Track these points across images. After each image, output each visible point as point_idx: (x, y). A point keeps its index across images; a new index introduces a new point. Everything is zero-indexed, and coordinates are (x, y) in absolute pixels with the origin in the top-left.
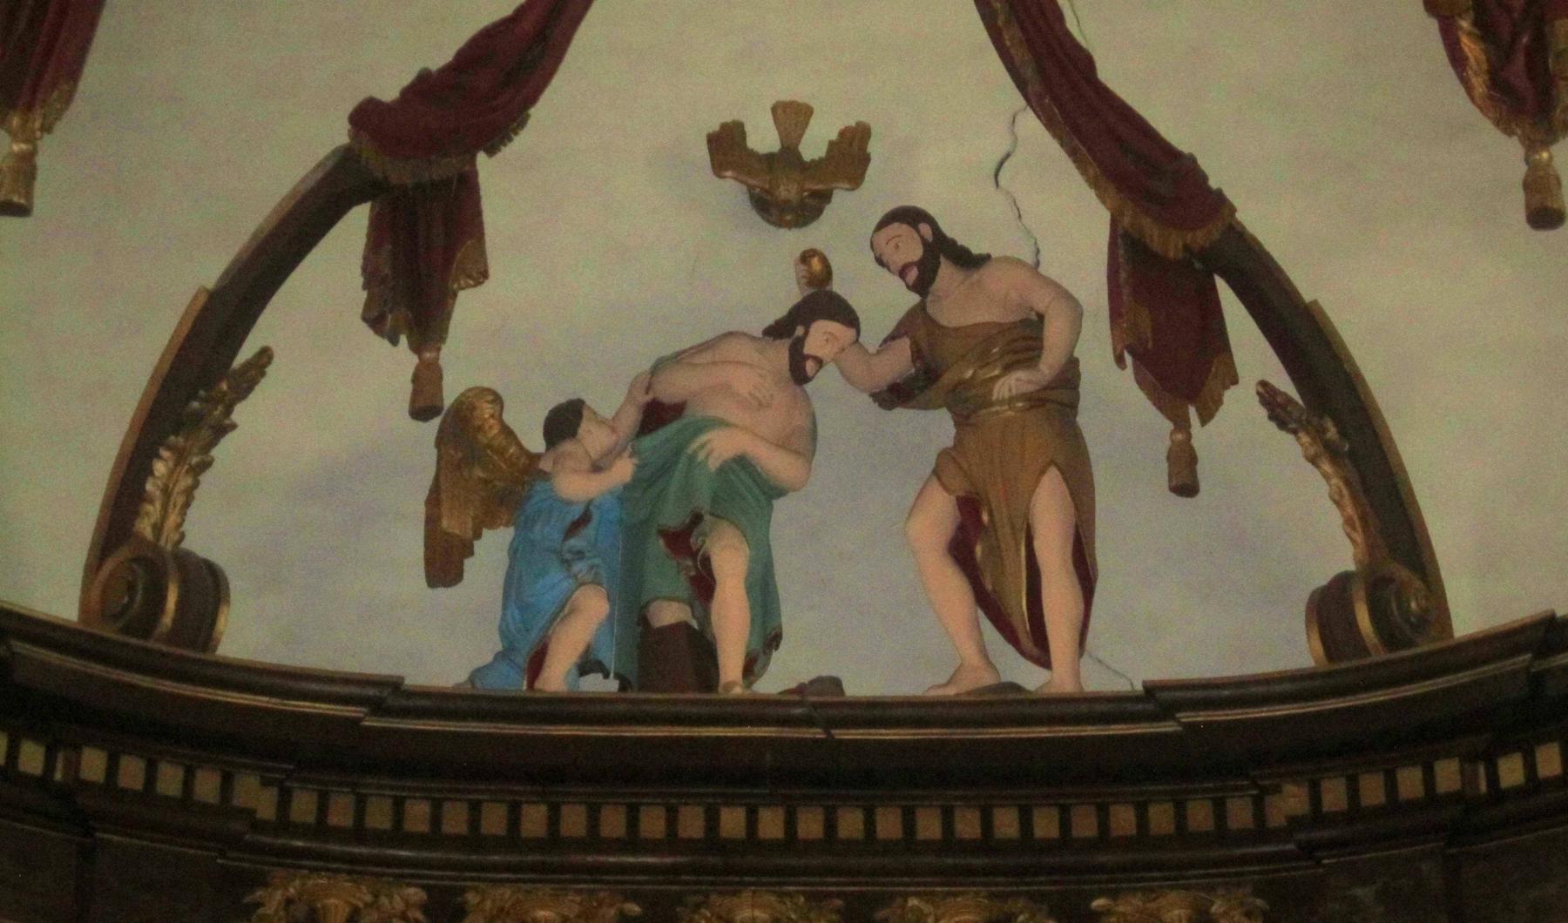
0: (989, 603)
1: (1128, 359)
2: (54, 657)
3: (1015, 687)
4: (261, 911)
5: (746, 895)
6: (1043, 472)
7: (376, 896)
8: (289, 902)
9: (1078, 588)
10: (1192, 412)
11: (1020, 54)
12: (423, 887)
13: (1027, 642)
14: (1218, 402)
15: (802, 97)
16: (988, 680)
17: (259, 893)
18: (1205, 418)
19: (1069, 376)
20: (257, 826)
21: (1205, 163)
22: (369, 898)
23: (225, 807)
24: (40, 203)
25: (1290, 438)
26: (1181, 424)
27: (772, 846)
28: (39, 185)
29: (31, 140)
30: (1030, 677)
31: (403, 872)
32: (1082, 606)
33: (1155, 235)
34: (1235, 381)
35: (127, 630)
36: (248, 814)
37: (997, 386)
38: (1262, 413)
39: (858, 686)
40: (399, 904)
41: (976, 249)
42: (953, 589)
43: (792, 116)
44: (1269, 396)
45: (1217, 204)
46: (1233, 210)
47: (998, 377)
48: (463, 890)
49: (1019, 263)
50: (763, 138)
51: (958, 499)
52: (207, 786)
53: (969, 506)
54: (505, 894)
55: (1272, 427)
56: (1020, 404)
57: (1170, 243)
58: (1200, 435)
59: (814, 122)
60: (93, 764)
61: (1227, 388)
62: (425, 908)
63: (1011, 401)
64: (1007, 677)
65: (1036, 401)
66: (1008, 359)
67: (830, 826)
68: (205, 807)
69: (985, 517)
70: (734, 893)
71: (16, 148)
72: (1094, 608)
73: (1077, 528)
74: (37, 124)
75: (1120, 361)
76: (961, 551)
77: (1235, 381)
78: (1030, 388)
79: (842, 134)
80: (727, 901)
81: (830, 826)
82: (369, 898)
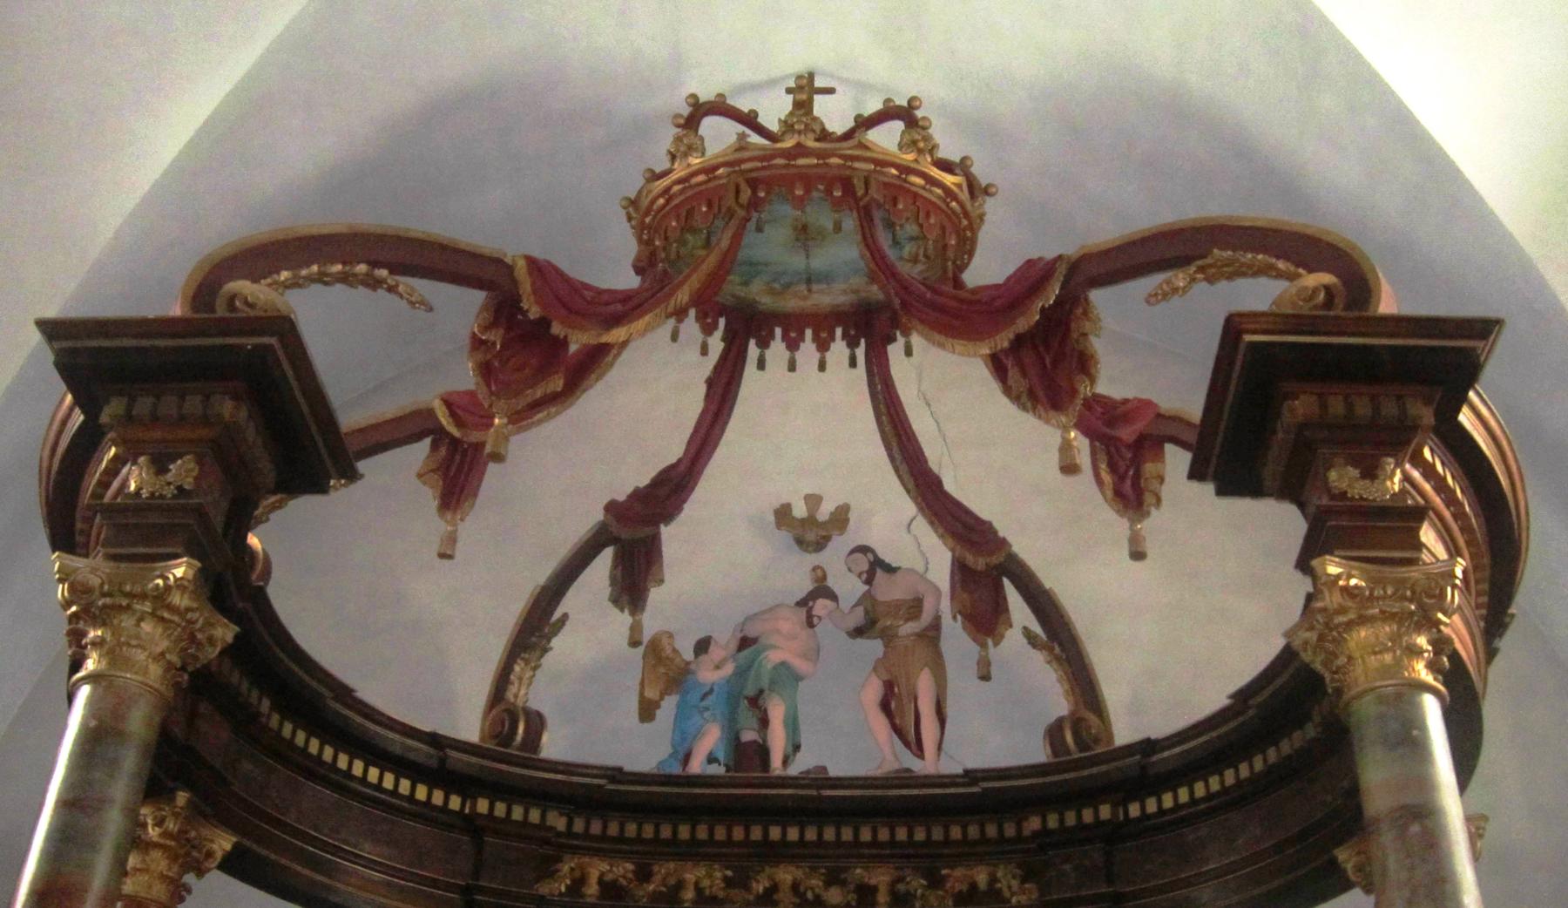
0: (898, 730)
1: (959, 617)
2: (465, 757)
3: (908, 770)
4: (558, 874)
5: (782, 866)
6: (922, 670)
7: (611, 866)
8: (572, 869)
9: (938, 725)
10: (990, 642)
11: (906, 477)
12: (633, 863)
13: (913, 746)
14: (1002, 637)
15: (817, 492)
16: (896, 766)
17: (561, 865)
18: (996, 644)
19: (936, 626)
20: (559, 834)
21: (997, 525)
22: (608, 868)
23: (542, 826)
24: (459, 555)
25: (1039, 652)
26: (983, 646)
27: (793, 844)
28: (459, 545)
29: (455, 525)
30: (920, 767)
31: (626, 855)
32: (939, 734)
33: (970, 559)
34: (1011, 626)
35: (498, 745)
36: (552, 829)
37: (901, 628)
38: (1025, 641)
39: (833, 772)
40: (622, 871)
41: (894, 565)
42: (880, 724)
43: (813, 501)
44: (1028, 633)
45: (1003, 543)
46: (1010, 546)
47: (901, 625)
48: (650, 865)
49: (916, 573)
50: (800, 511)
51: (884, 682)
52: (535, 816)
53: (889, 686)
54: (672, 865)
55: (1029, 647)
56: (912, 638)
57: (979, 563)
58: (994, 652)
59: (824, 503)
60: (483, 806)
61: (1007, 629)
62: (633, 872)
63: (908, 636)
64: (906, 765)
65: (921, 635)
66: (907, 616)
67: (820, 835)
68: (535, 826)
69: (896, 690)
70: (777, 866)
71: (449, 528)
72: (946, 732)
73: (938, 696)
74: (459, 517)
75: (954, 618)
76: (885, 706)
77: (1011, 626)
78: (917, 630)
79: (837, 508)
80: (774, 870)
81: (820, 835)
82: (608, 868)
